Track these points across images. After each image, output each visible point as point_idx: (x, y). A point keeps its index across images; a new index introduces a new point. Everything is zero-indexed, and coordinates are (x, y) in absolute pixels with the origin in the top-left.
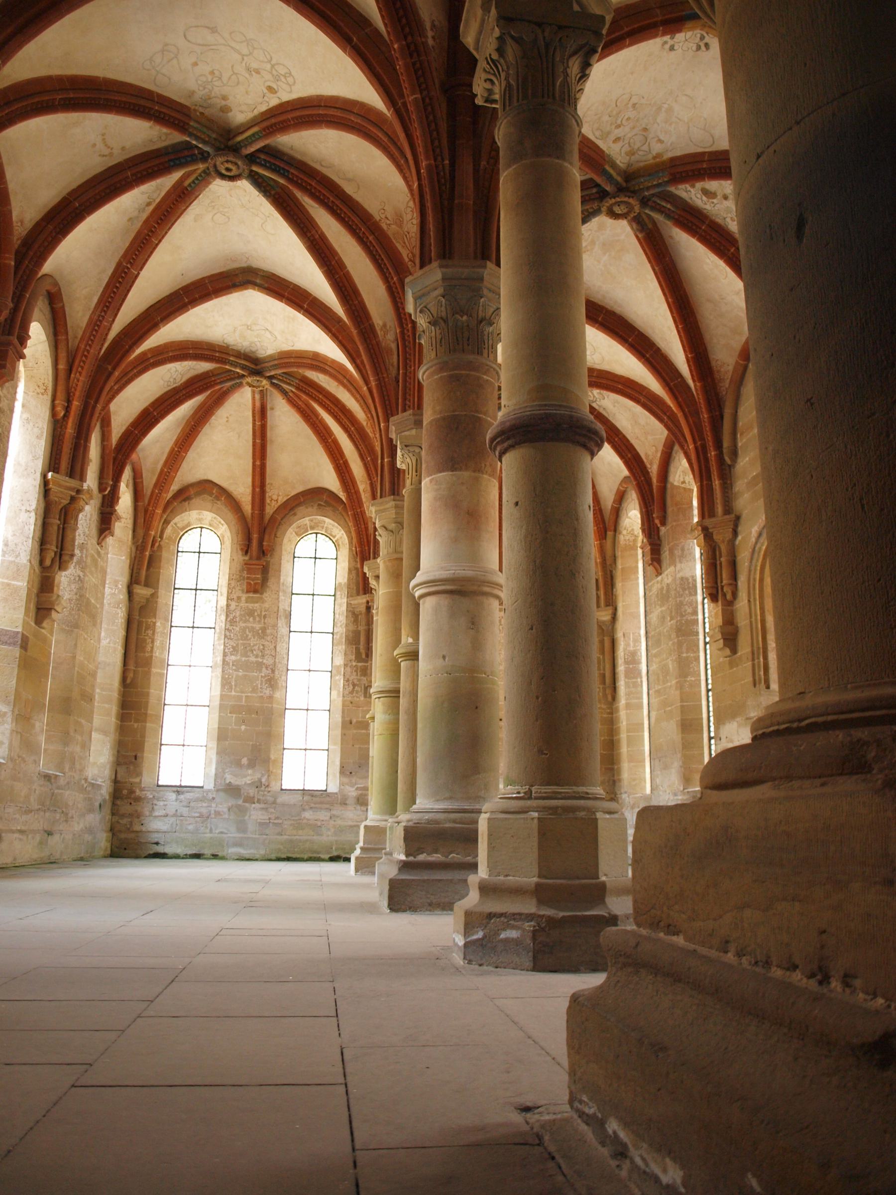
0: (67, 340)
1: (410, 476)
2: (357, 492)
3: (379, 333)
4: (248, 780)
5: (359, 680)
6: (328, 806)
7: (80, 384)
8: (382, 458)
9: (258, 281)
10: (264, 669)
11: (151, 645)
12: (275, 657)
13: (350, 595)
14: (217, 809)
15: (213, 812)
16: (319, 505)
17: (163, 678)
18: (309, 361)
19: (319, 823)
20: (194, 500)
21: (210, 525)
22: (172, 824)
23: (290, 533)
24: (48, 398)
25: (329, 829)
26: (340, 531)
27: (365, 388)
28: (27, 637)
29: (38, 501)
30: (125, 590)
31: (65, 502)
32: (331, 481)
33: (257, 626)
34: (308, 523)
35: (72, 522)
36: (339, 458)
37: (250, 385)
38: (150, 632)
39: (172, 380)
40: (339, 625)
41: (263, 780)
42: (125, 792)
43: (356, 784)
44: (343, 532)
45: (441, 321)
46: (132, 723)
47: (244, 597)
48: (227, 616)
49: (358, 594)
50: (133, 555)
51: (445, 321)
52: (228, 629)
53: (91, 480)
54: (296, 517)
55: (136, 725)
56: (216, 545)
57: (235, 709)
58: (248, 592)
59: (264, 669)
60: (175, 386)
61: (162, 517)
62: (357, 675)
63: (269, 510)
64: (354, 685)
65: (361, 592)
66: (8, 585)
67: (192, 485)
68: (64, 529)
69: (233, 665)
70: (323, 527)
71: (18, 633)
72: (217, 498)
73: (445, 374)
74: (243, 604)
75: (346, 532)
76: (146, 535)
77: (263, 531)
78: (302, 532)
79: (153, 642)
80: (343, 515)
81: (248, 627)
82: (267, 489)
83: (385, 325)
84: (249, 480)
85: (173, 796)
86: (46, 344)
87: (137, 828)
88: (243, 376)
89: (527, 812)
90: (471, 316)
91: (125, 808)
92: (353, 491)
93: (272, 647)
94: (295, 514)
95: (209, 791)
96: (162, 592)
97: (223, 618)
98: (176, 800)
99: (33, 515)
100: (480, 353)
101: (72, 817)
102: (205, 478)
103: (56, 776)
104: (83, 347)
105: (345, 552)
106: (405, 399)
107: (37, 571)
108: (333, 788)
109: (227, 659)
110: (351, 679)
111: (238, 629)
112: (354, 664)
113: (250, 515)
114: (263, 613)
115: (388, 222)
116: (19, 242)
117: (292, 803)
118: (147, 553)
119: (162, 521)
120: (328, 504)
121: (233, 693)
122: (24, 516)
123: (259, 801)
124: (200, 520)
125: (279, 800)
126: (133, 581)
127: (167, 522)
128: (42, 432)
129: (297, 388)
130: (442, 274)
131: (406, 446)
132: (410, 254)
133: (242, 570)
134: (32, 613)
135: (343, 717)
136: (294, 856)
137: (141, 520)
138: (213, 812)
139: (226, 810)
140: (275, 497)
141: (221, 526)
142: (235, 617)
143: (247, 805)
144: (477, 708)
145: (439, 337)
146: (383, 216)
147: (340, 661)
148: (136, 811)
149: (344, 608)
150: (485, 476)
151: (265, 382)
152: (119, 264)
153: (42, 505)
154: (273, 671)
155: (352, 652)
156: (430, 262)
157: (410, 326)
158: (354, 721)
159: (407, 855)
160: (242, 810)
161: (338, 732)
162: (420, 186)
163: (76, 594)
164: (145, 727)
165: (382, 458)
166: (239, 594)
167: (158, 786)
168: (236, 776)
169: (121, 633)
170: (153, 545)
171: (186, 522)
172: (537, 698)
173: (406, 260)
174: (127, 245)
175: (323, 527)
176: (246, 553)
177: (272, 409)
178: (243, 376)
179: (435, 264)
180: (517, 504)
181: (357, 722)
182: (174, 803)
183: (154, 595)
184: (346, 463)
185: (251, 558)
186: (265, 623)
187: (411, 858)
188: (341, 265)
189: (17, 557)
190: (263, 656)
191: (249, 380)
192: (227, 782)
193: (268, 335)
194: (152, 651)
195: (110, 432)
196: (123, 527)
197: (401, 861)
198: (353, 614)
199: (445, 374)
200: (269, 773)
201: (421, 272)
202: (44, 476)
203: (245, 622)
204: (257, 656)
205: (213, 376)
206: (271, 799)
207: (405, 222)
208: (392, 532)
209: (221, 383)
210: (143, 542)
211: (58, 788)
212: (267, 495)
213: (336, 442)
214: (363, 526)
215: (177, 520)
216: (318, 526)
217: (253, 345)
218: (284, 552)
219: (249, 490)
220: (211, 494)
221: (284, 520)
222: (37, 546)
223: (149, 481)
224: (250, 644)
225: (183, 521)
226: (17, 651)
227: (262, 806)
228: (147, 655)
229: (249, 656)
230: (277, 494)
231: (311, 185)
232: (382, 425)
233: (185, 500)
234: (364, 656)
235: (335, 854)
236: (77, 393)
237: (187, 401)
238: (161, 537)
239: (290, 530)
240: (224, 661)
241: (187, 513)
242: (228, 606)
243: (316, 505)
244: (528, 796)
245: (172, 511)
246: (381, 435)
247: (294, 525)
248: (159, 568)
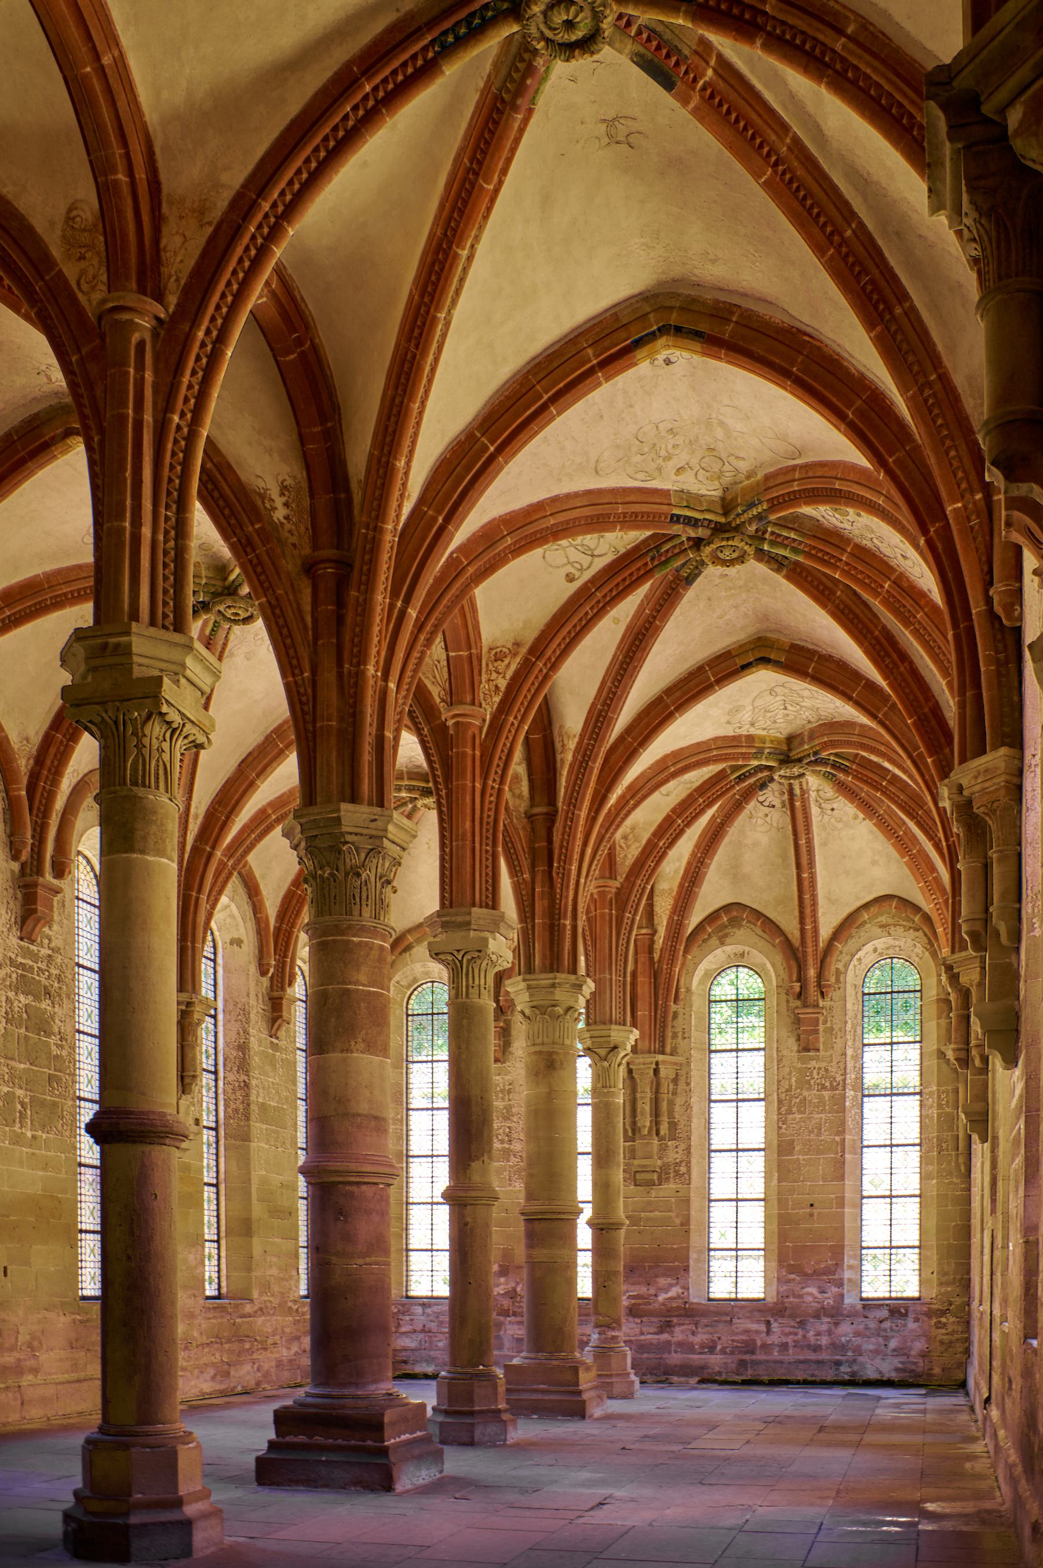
20: (414, 951)
43: (627, 1291)
85: (419, 1310)
98: (424, 1313)
114: (507, 1088)
123: (515, 1314)
143: (502, 1318)
167: (407, 1297)
204: (502, 1142)
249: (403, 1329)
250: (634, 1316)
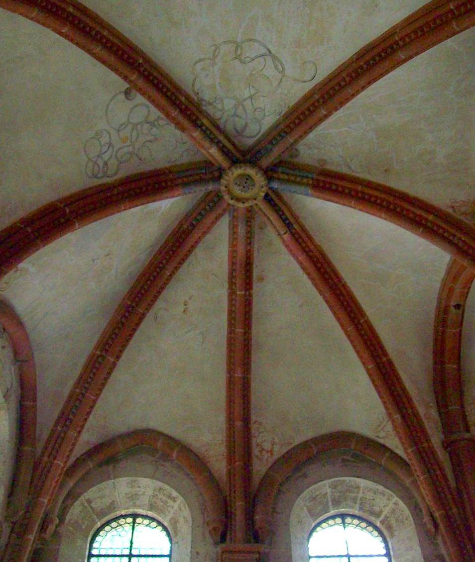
16: (344, 460)
21: (152, 507)
23: (300, 507)
34: (329, 490)
44: (396, 499)
63: (260, 468)
67: (120, 437)
72: (166, 457)
75: (402, 498)
77: (251, 502)
82: (254, 428)
84: (221, 419)
92: (410, 411)
94: (305, 476)
113: (225, 478)
118: (31, 537)
124: (133, 498)
127: (72, 496)
137: (25, 477)
140: (267, 446)
141: (171, 503)
170: (43, 528)
171: (107, 501)
177: (261, 279)
210: (25, 518)
212: (254, 441)
215: (91, 493)
216: (345, 499)
225: (102, 497)
239: (299, 501)
241: (110, 482)
243: (340, 460)
245: (83, 479)
247: (306, 493)
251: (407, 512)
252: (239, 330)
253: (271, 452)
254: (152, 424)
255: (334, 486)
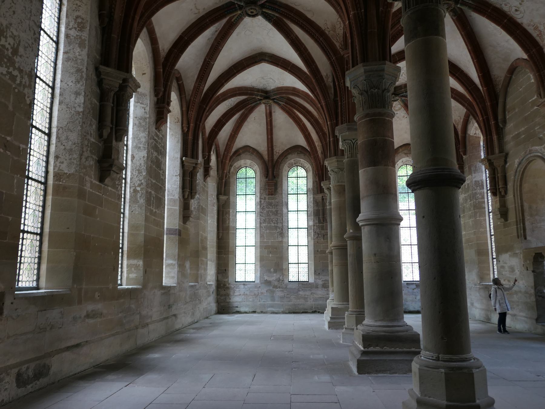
0: (186, 97)
1: (347, 154)
2: (315, 147)
3: (324, 79)
4: (274, 278)
5: (320, 232)
6: (310, 289)
7: (193, 116)
8: (329, 138)
9: (267, 59)
10: (278, 229)
11: (228, 221)
12: (282, 223)
13: (314, 194)
14: (261, 291)
15: (260, 293)
16: (298, 153)
17: (235, 234)
18: (291, 92)
19: (306, 296)
22: (243, 299)
23: (286, 167)
24: (180, 124)
25: (311, 299)
26: (308, 164)
27: (319, 105)
28: (181, 230)
29: (180, 170)
30: (216, 198)
31: (191, 169)
32: (302, 141)
33: (274, 210)
34: (293, 161)
35: (195, 177)
36: (306, 131)
37: (264, 103)
38: (228, 215)
39: (230, 105)
40: (310, 207)
41: (281, 278)
42: (222, 285)
44: (309, 165)
45: (365, 93)
46: (223, 255)
47: (267, 197)
48: (260, 206)
49: (318, 193)
50: (218, 182)
51: (366, 92)
52: (261, 212)
53: (200, 159)
54: (288, 160)
55: (224, 256)
56: (253, 175)
57: (267, 247)
58: (269, 195)
59: (278, 229)
60: (231, 107)
61: (229, 163)
62: (319, 230)
63: (275, 158)
64: (318, 234)
65: (319, 192)
66: (171, 209)
68: (191, 181)
69: (264, 228)
70: (300, 163)
71: (177, 229)
72: (252, 154)
73: (368, 119)
74: (267, 200)
76: (223, 172)
78: (291, 167)
79: (229, 219)
80: (308, 157)
81: (269, 211)
82: (274, 148)
83: (327, 75)
85: (242, 286)
86: (177, 100)
87: (228, 301)
88: (261, 100)
89: (438, 369)
90: (379, 89)
91: (223, 292)
92: (313, 146)
93: (281, 219)
94: (287, 158)
95: (257, 284)
96: (231, 197)
97: (259, 207)
98: (244, 288)
99: (178, 177)
100: (384, 107)
101: (202, 301)
102: (246, 145)
103: (195, 285)
104: (192, 99)
105: (311, 174)
106: (342, 117)
107: (182, 200)
108: (312, 281)
109: (262, 225)
110: (317, 231)
111: (265, 212)
112: (318, 225)
113: (267, 161)
114: (276, 204)
115: (329, 30)
116: (163, 59)
117: (294, 288)
118: (224, 181)
119: (229, 165)
120: (301, 152)
121: (265, 240)
122: (175, 178)
123: (279, 287)
125: (288, 287)
126: (219, 194)
127: (231, 166)
128: (179, 140)
129: (286, 103)
130: (364, 69)
131: (344, 140)
132: (340, 45)
133: (265, 185)
134: (181, 220)
135: (314, 249)
136: (296, 311)
137: (220, 166)
138: (260, 293)
139: (265, 292)
140: (278, 151)
142: (264, 207)
143: (274, 289)
144: (392, 278)
145: (364, 100)
146: (326, 27)
147: (311, 223)
148: (227, 293)
149: (312, 199)
150: (390, 167)
151: (271, 101)
152: (205, 60)
153: (182, 172)
154: (282, 230)
155: (317, 219)
156: (357, 64)
157: (342, 81)
158: (319, 250)
159: (364, 348)
160: (272, 292)
161: (313, 256)
162: (349, 23)
163: (197, 205)
164: (228, 257)
165: (329, 138)
166: (265, 196)
167: (236, 282)
168: (268, 276)
169: (216, 217)
170: (226, 177)
171: (239, 165)
172: (440, 313)
173: (339, 48)
174: (208, 51)
175: (300, 163)
176: (267, 177)
178: (261, 100)
179: (360, 65)
180: (424, 217)
181: (321, 251)
182: (244, 289)
183: (228, 199)
184: (309, 134)
185: (269, 180)
186: (277, 208)
187: (366, 349)
188: (306, 49)
189: (173, 196)
190: (277, 223)
191: (264, 101)
192: (265, 279)
193: (271, 80)
194: (229, 223)
195: (205, 131)
196: (213, 172)
197: (362, 351)
198: (316, 202)
199: (368, 119)
200: (283, 275)
201: (353, 69)
202: (181, 159)
203: (268, 208)
204: (274, 223)
205: (248, 101)
206: (284, 286)
207: (337, 29)
208: (336, 172)
209: (252, 103)
211: (197, 290)
213: (304, 125)
214: (318, 162)
215: (235, 165)
217: (265, 85)
218: (283, 176)
219: (266, 149)
220: (249, 152)
221: (283, 161)
222: (181, 190)
223: (222, 148)
224: (271, 218)
226: (177, 237)
227: (281, 289)
228: (227, 225)
229: (271, 224)
230: (279, 149)
231: (291, 15)
232: (328, 123)
233: (238, 155)
234: (322, 221)
235: (314, 310)
236: (192, 120)
237: (237, 114)
238: (229, 173)
239: (286, 165)
240: (260, 226)
242: (260, 202)
244: (438, 359)
245: (233, 161)
246: (328, 127)
248: (229, 187)
249: (236, 294)
250: (325, 288)
251: (311, 169)
252: (269, 127)
253: (279, 153)
254: (248, 144)
255: (294, 160)
